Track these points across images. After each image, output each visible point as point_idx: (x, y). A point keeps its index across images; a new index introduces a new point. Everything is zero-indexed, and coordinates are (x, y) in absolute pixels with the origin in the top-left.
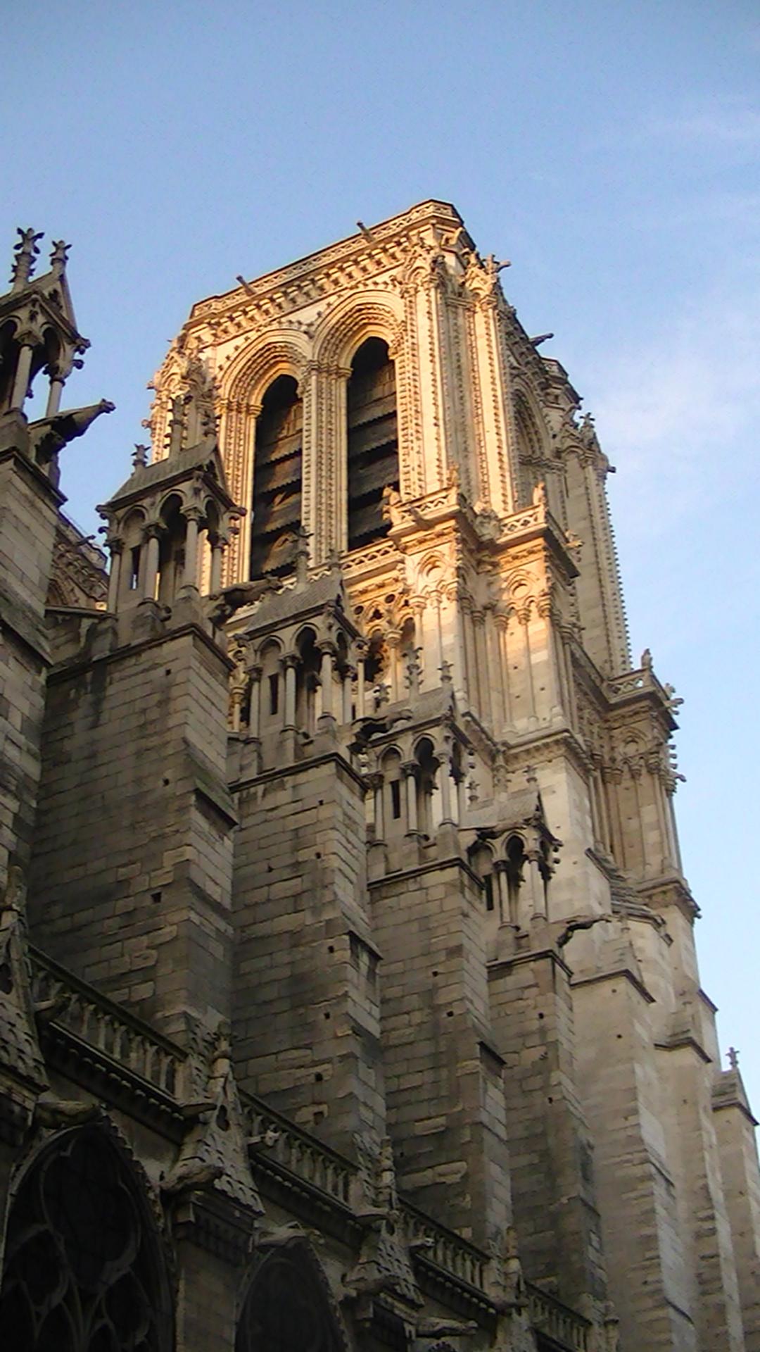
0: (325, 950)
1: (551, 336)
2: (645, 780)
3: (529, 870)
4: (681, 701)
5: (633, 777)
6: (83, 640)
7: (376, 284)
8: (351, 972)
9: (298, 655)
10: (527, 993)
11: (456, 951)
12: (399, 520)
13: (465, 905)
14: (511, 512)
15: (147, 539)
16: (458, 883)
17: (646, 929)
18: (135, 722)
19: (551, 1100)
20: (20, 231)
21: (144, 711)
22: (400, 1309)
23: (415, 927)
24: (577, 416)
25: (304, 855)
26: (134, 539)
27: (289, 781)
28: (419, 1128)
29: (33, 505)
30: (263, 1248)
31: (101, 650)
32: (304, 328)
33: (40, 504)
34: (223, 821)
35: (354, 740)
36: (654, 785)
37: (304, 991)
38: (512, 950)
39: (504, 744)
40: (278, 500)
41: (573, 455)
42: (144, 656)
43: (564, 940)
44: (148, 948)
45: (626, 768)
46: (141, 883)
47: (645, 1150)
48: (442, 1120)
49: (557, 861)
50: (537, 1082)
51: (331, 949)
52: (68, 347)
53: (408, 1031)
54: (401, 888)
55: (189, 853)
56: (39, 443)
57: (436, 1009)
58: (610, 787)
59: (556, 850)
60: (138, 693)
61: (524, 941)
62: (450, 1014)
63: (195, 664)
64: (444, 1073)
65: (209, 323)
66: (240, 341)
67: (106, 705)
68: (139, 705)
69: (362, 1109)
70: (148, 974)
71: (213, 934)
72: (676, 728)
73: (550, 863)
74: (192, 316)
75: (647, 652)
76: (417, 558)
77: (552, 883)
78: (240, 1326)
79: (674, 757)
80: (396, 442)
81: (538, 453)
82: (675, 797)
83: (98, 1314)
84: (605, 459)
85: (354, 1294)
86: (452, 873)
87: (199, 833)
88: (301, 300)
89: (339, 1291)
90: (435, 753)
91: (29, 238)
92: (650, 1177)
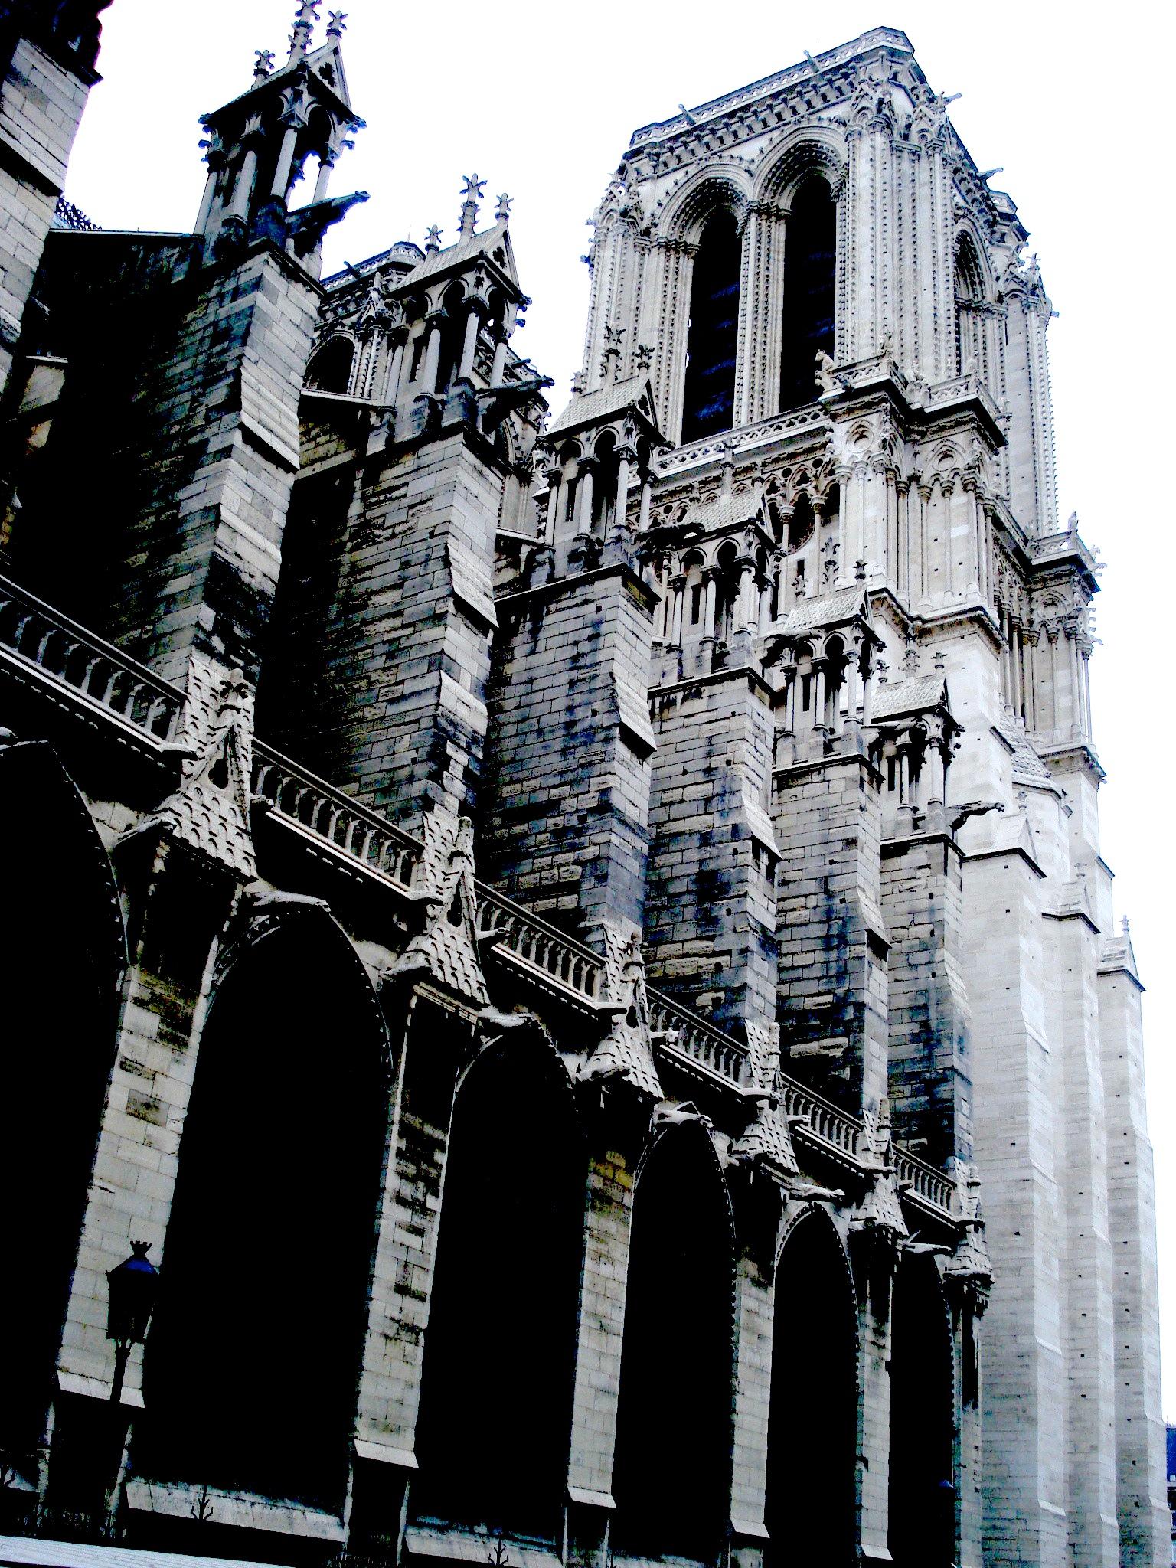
0: (731, 851)
3: (932, 755)
4: (1103, 566)
5: (1050, 640)
6: (523, 565)
7: (820, 119)
8: (751, 874)
11: (851, 843)
12: (831, 390)
13: (864, 801)
14: (943, 378)
15: (581, 475)
18: (571, 652)
19: (934, 975)
21: (576, 643)
22: (777, 1176)
23: (816, 816)
24: (1025, 254)
25: (717, 762)
26: (571, 470)
27: (707, 690)
28: (809, 1003)
29: (480, 473)
30: (660, 1127)
31: (539, 581)
32: (745, 165)
33: (486, 471)
34: (640, 749)
37: (712, 886)
42: (579, 591)
43: (957, 824)
44: (574, 863)
45: (1043, 631)
46: (569, 804)
48: (829, 998)
49: (958, 746)
50: (921, 957)
52: (512, 307)
53: (805, 912)
54: (808, 779)
55: (612, 781)
57: (830, 895)
58: (1026, 648)
59: (958, 735)
61: (920, 823)
62: (843, 901)
63: (623, 602)
64: (834, 955)
66: (680, 176)
67: (542, 635)
68: (571, 638)
69: (755, 996)
70: (573, 887)
73: (951, 748)
74: (632, 142)
76: (846, 426)
77: (950, 768)
79: (1094, 619)
81: (980, 297)
85: (737, 1163)
86: (854, 770)
87: (623, 762)
88: (743, 134)
89: (724, 1159)
90: (846, 651)
91: (473, 185)
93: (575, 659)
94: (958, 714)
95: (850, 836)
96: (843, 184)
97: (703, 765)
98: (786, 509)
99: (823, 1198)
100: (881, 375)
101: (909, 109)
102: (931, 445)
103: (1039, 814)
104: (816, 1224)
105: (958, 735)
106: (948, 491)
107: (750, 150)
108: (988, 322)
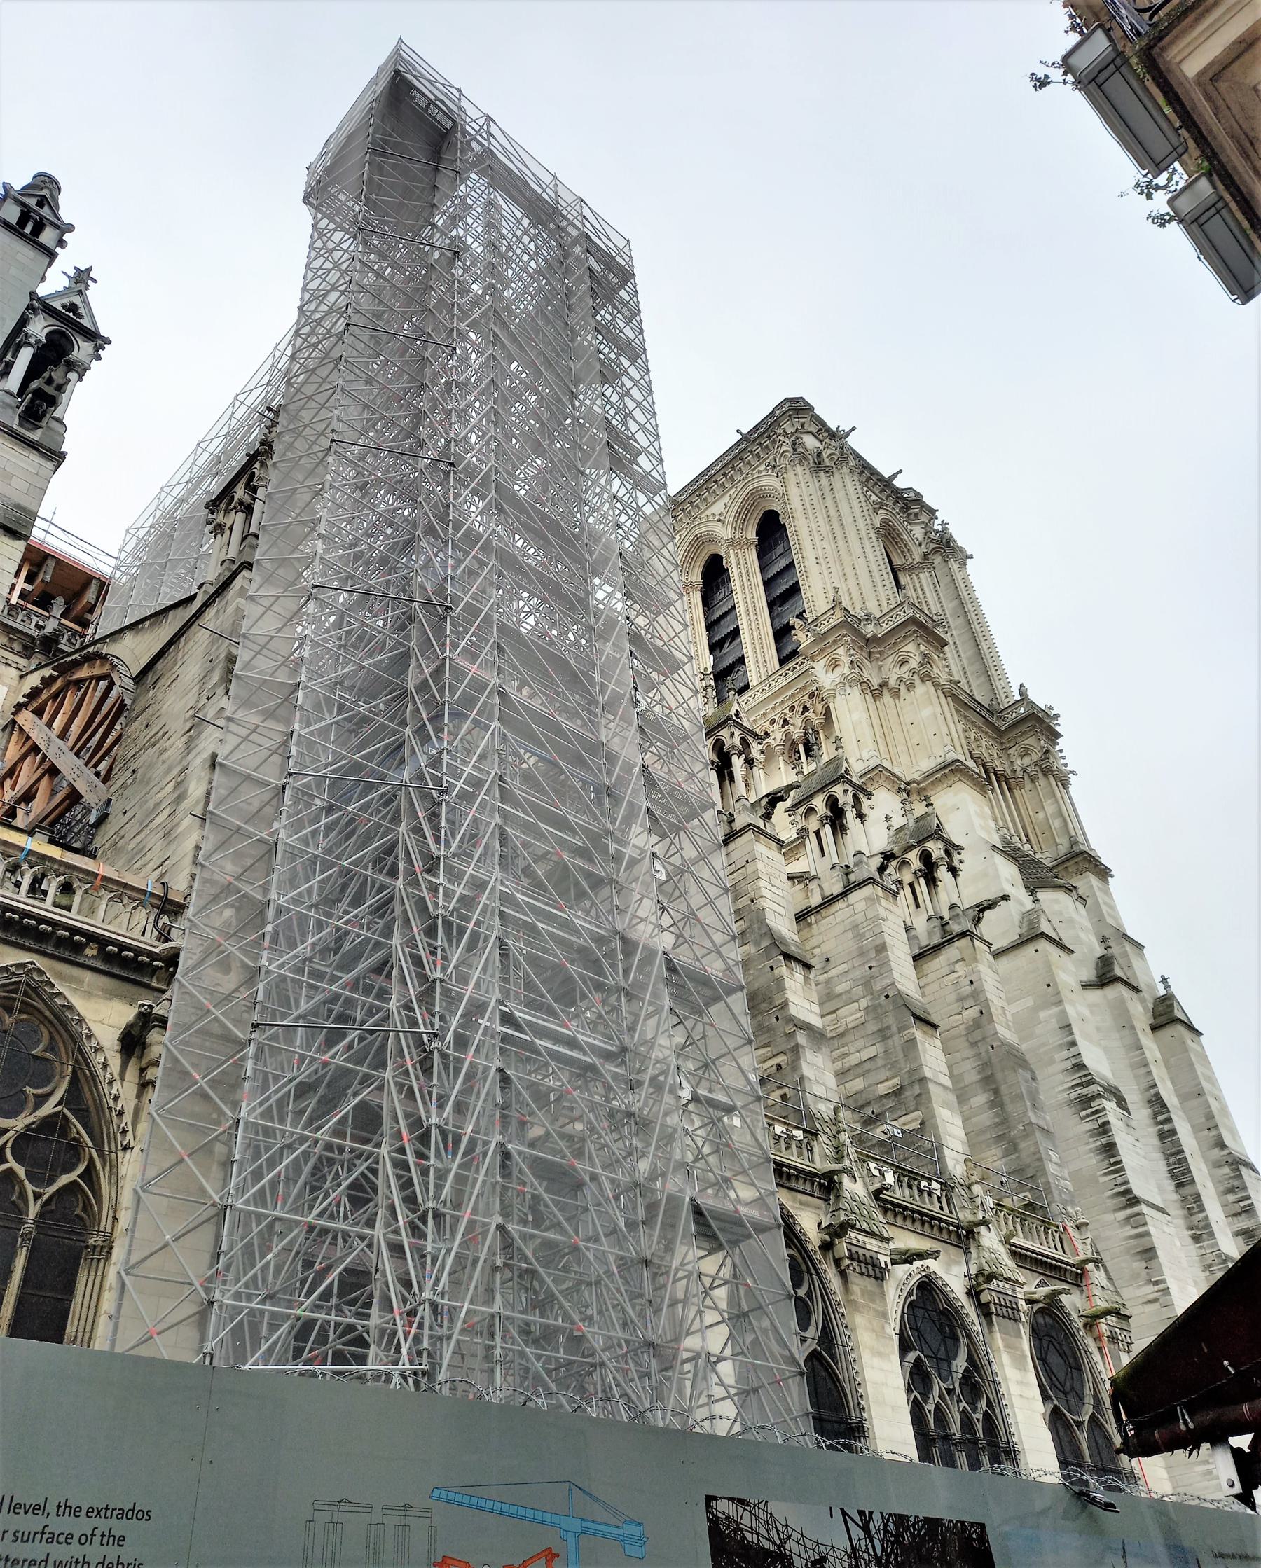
3: (943, 873)
5: (1033, 781)
9: (716, 759)
10: (957, 967)
39: (913, 781)
43: (977, 921)
45: (1026, 777)
48: (897, 1080)
51: (772, 968)
58: (1017, 793)
62: (887, 997)
72: (1058, 735)
75: (1022, 685)
79: (1064, 758)
82: (1071, 788)
84: (962, 550)
86: (868, 890)
92: (1099, 1096)
95: (878, 942)
96: (785, 508)
98: (798, 734)
101: (818, 444)
102: (890, 659)
103: (1056, 907)
107: (718, 508)
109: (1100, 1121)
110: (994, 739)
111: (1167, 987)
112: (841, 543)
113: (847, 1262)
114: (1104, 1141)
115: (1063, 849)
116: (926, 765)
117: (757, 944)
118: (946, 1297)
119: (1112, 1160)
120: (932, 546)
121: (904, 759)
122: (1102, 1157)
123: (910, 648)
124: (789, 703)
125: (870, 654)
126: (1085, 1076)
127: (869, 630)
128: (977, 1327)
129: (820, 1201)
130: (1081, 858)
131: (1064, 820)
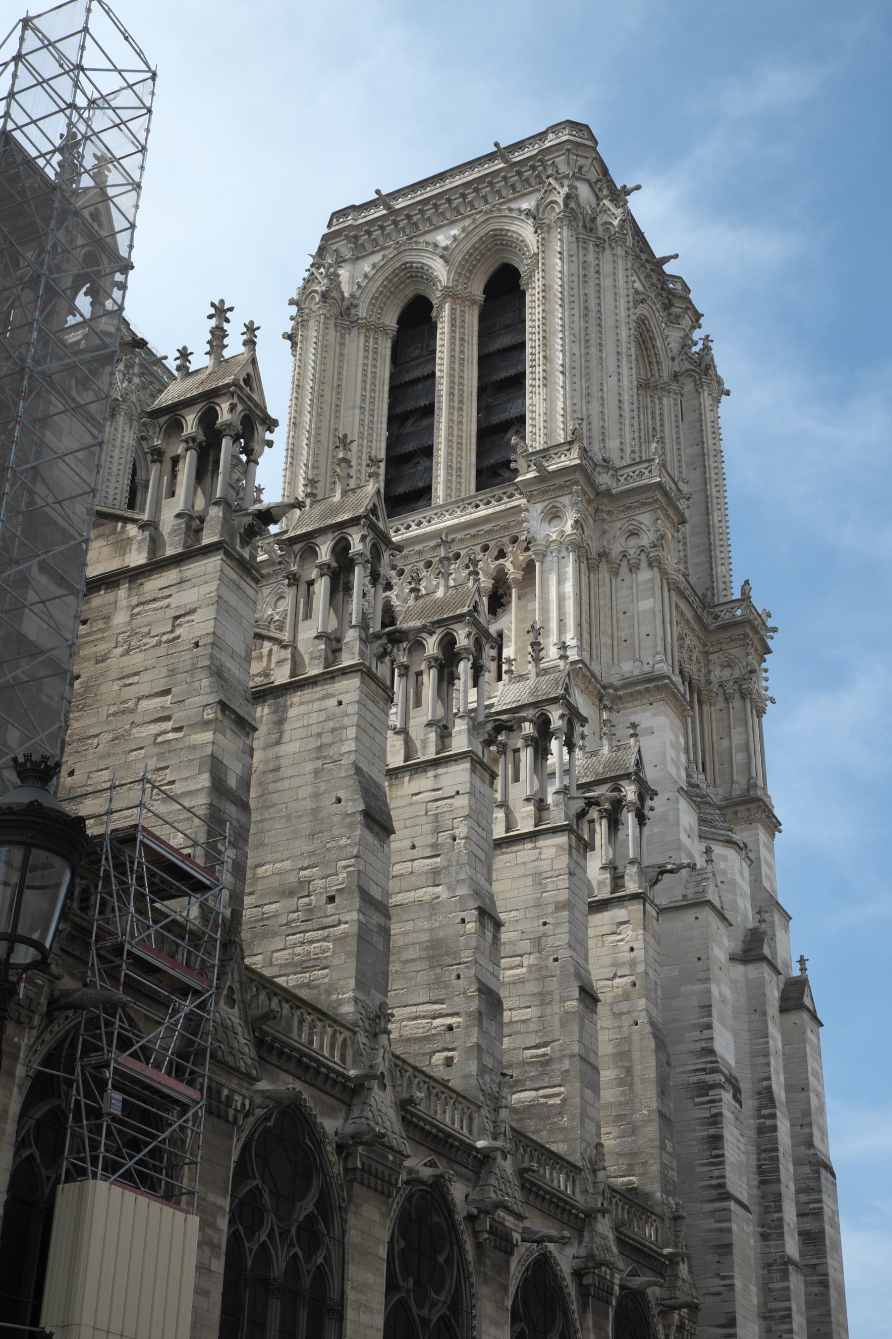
1: (676, 256)
2: (737, 703)
4: (775, 630)
5: (727, 700)
16: (567, 846)
17: (731, 854)
20: (213, 305)
21: (319, 734)
24: (697, 335)
29: (238, 586)
33: (243, 585)
35: (486, 737)
36: (745, 708)
38: (609, 889)
39: (611, 686)
40: (410, 422)
41: (691, 379)
45: (720, 692)
47: (716, 1062)
49: (652, 809)
52: (260, 428)
56: (242, 531)
58: (705, 708)
59: (652, 799)
60: (314, 718)
65: (347, 236)
67: (287, 726)
68: (315, 729)
71: (376, 930)
72: (768, 651)
75: (747, 582)
78: (391, 1243)
79: (766, 680)
80: (523, 374)
82: (765, 718)
83: (291, 1245)
84: (720, 382)
85: (475, 1212)
89: (461, 1210)
92: (720, 1086)
93: (319, 748)
94: (650, 774)
97: (430, 840)
99: (551, 1239)
100: (570, 459)
102: (618, 524)
104: (542, 1267)
105: (652, 799)
106: (634, 568)
107: (442, 239)
108: (665, 400)
109: (714, 1111)
110: (699, 638)
111: (803, 969)
112: (594, 350)
113: (486, 1236)
114: (712, 1131)
115: (738, 790)
116: (628, 668)
117: (451, 888)
118: (555, 1275)
119: (715, 1152)
120: (687, 365)
121: (605, 653)
122: (705, 1147)
123: (645, 518)
124: (483, 540)
125: (597, 510)
126: (711, 1062)
127: (604, 479)
128: (574, 1307)
129: (471, 1174)
130: (755, 805)
131: (749, 757)
